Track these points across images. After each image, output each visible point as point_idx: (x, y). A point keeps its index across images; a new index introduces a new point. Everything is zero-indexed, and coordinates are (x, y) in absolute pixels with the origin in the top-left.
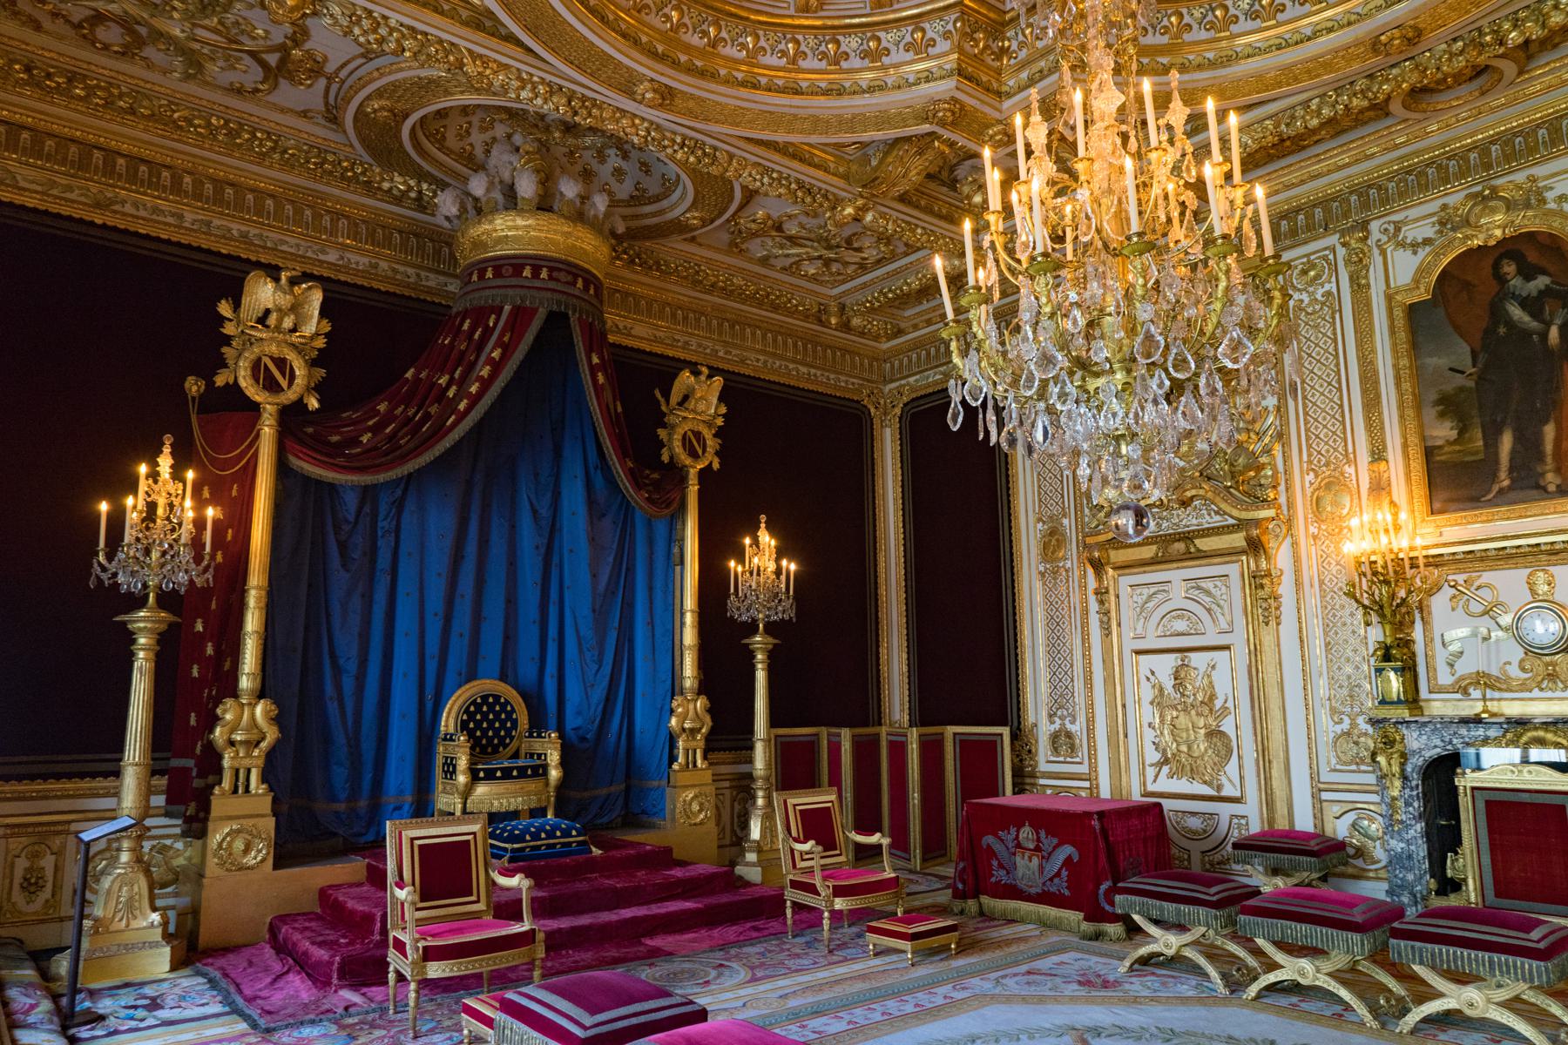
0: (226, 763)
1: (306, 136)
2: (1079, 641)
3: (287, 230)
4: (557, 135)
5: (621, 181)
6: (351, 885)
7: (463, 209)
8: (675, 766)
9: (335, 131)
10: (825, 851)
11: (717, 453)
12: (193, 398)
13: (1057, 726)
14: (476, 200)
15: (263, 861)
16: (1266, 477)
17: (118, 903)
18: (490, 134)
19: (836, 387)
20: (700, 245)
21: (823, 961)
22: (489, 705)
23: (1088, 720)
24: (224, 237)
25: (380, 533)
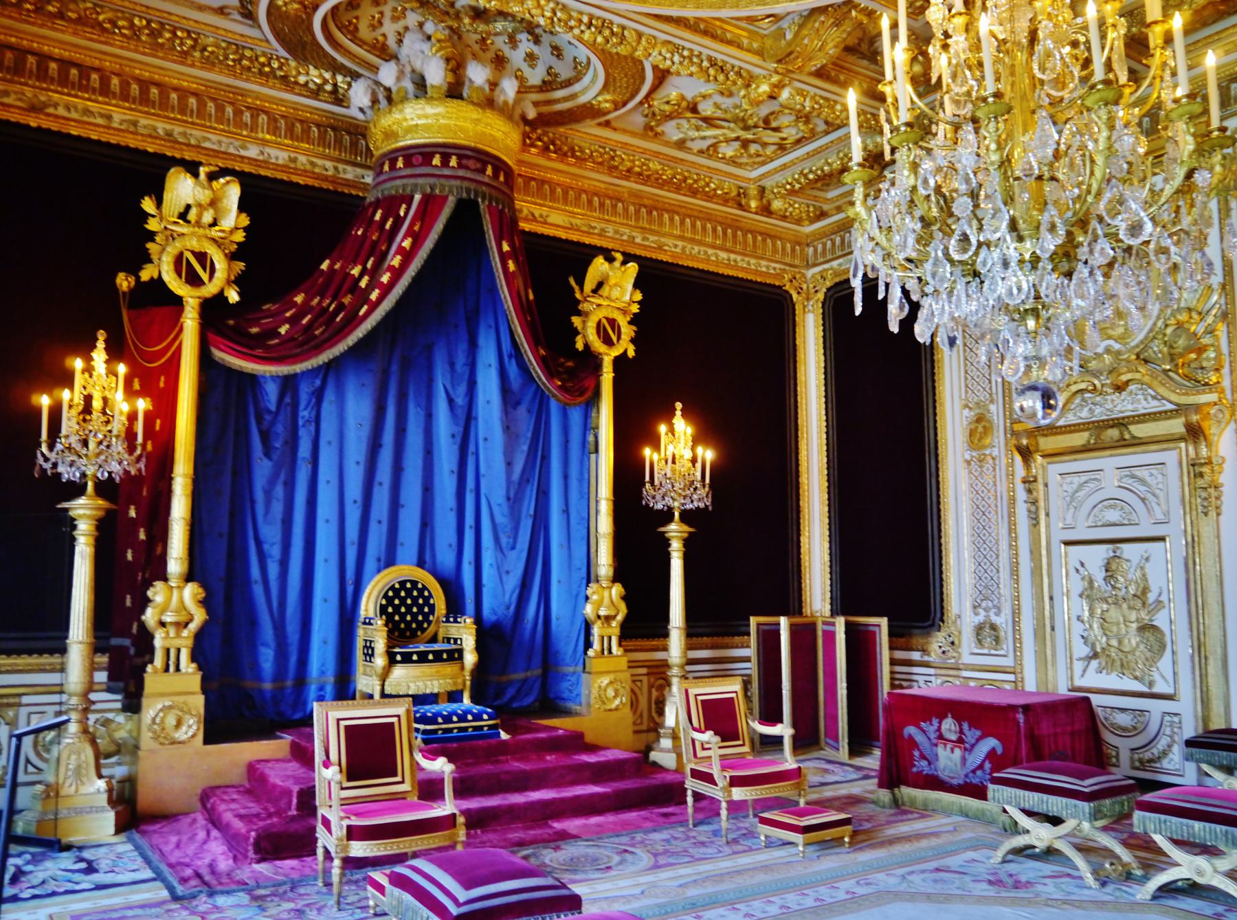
0: (158, 642)
1: (223, 33)
2: (1004, 531)
3: (210, 127)
4: (467, 21)
5: (532, 67)
6: (277, 761)
7: (375, 101)
8: (591, 653)
9: (251, 26)
10: (723, 741)
11: (633, 341)
12: (124, 293)
13: (981, 618)
14: (388, 90)
15: (193, 736)
16: (1208, 359)
17: (67, 770)
18: (402, 23)
19: (756, 272)
20: (615, 129)
21: (727, 850)
22: (407, 590)
23: (1014, 613)
24: (150, 136)
25: (301, 422)
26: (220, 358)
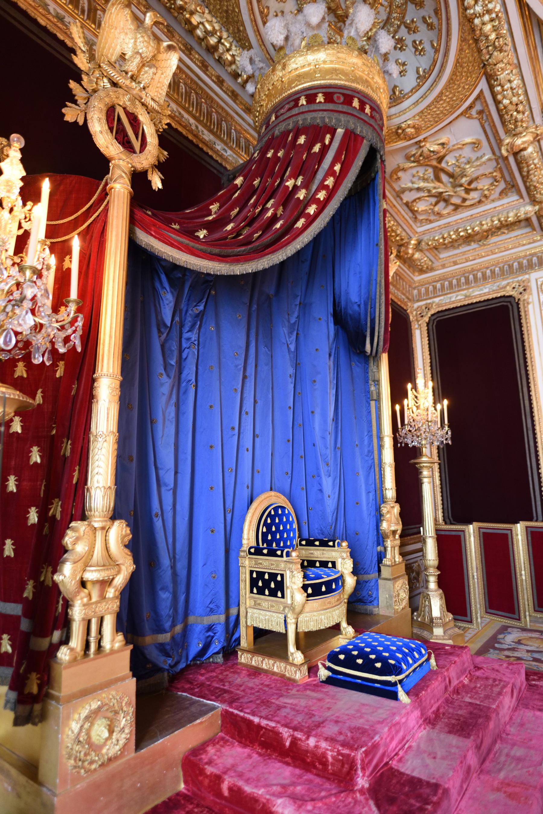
26: (147, 244)
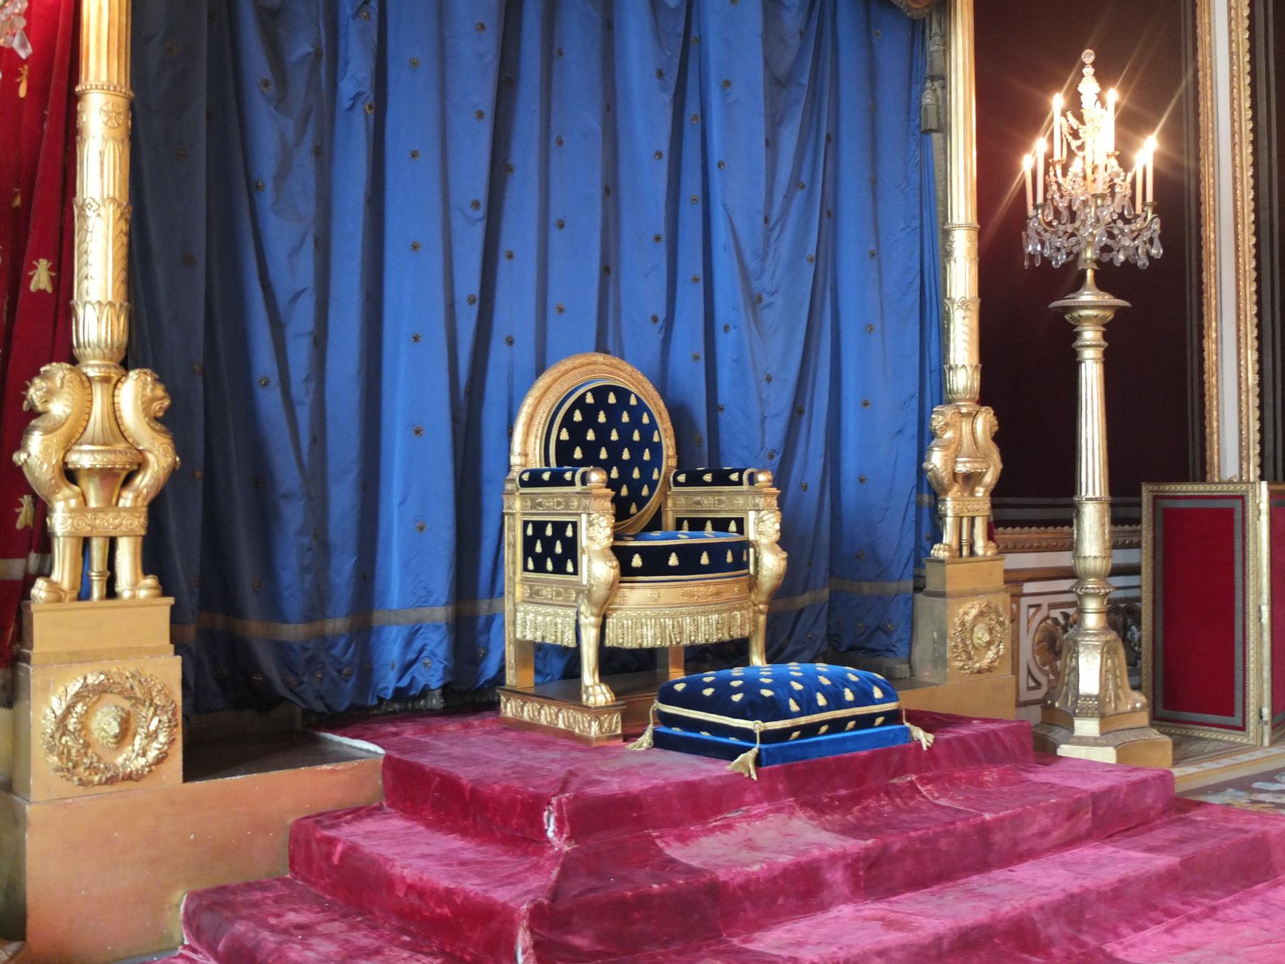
0: (60, 522)
8: (939, 552)
15: (159, 760)
